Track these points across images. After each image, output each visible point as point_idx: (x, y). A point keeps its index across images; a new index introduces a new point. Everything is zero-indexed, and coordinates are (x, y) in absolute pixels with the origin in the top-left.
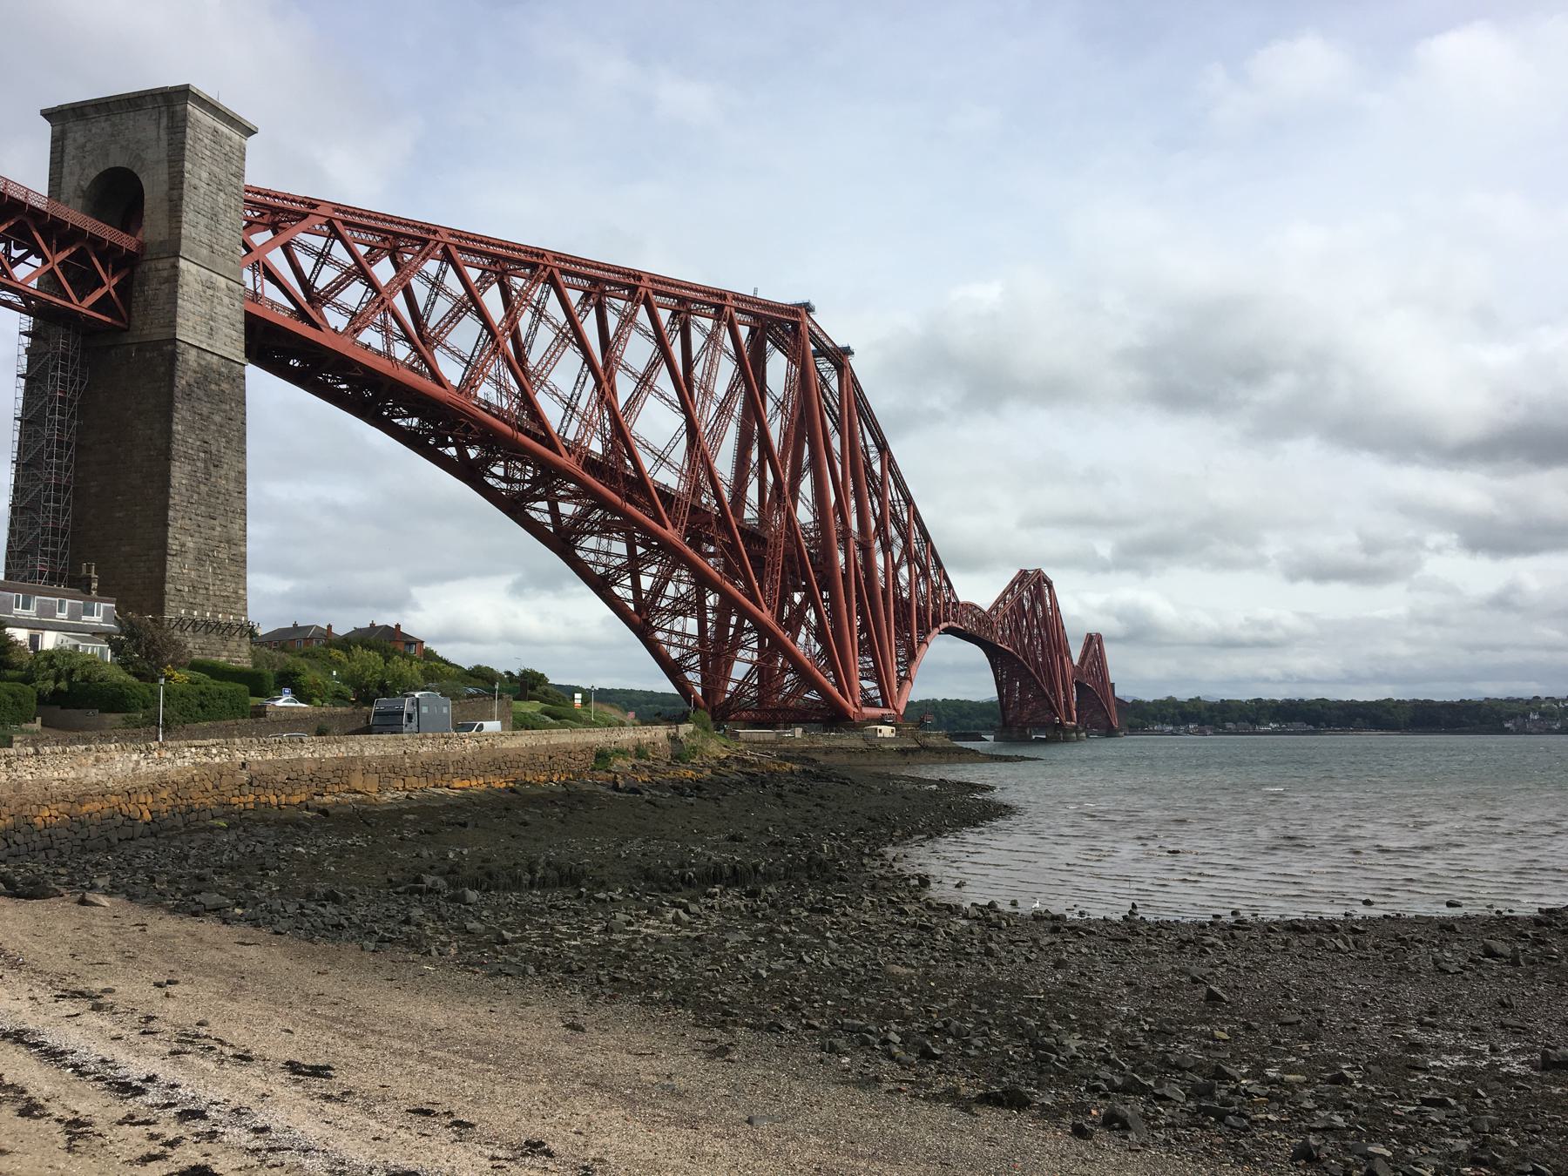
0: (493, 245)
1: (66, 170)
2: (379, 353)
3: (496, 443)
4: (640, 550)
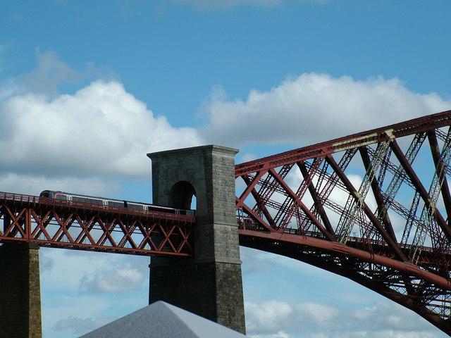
1: (160, 182)
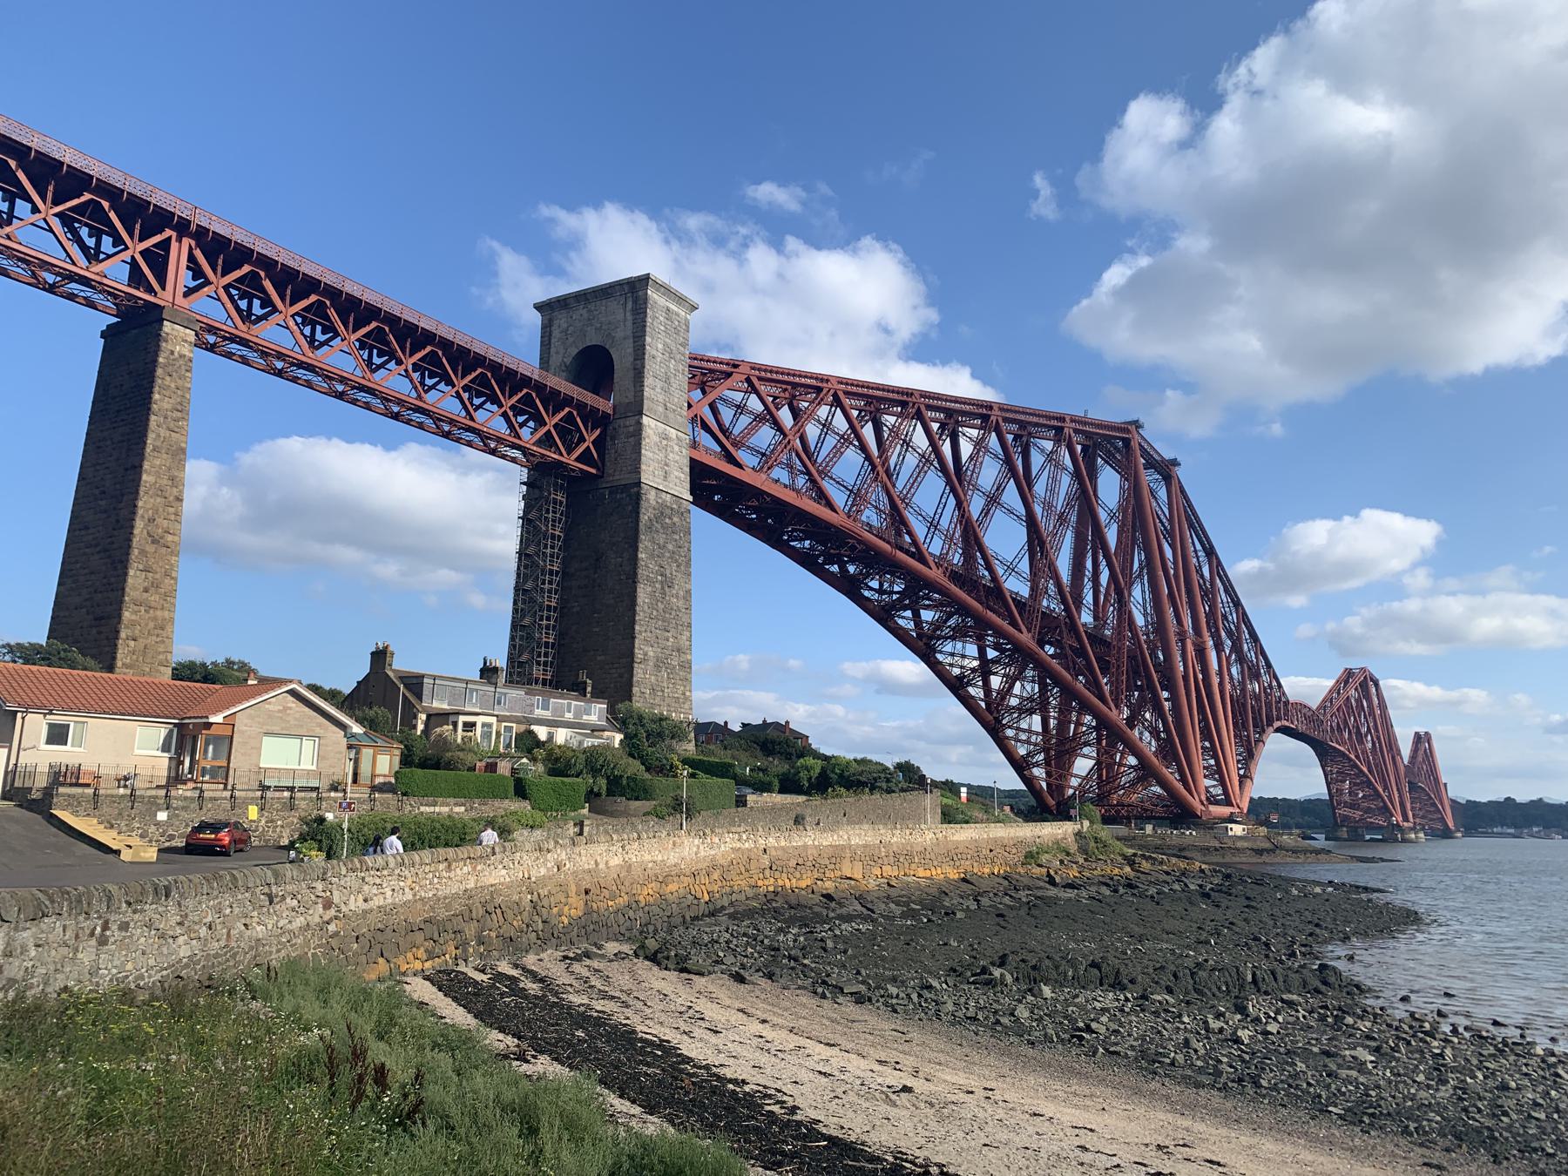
0: (872, 388)
1: (553, 350)
2: (786, 486)
3: (875, 561)
4: (991, 654)
